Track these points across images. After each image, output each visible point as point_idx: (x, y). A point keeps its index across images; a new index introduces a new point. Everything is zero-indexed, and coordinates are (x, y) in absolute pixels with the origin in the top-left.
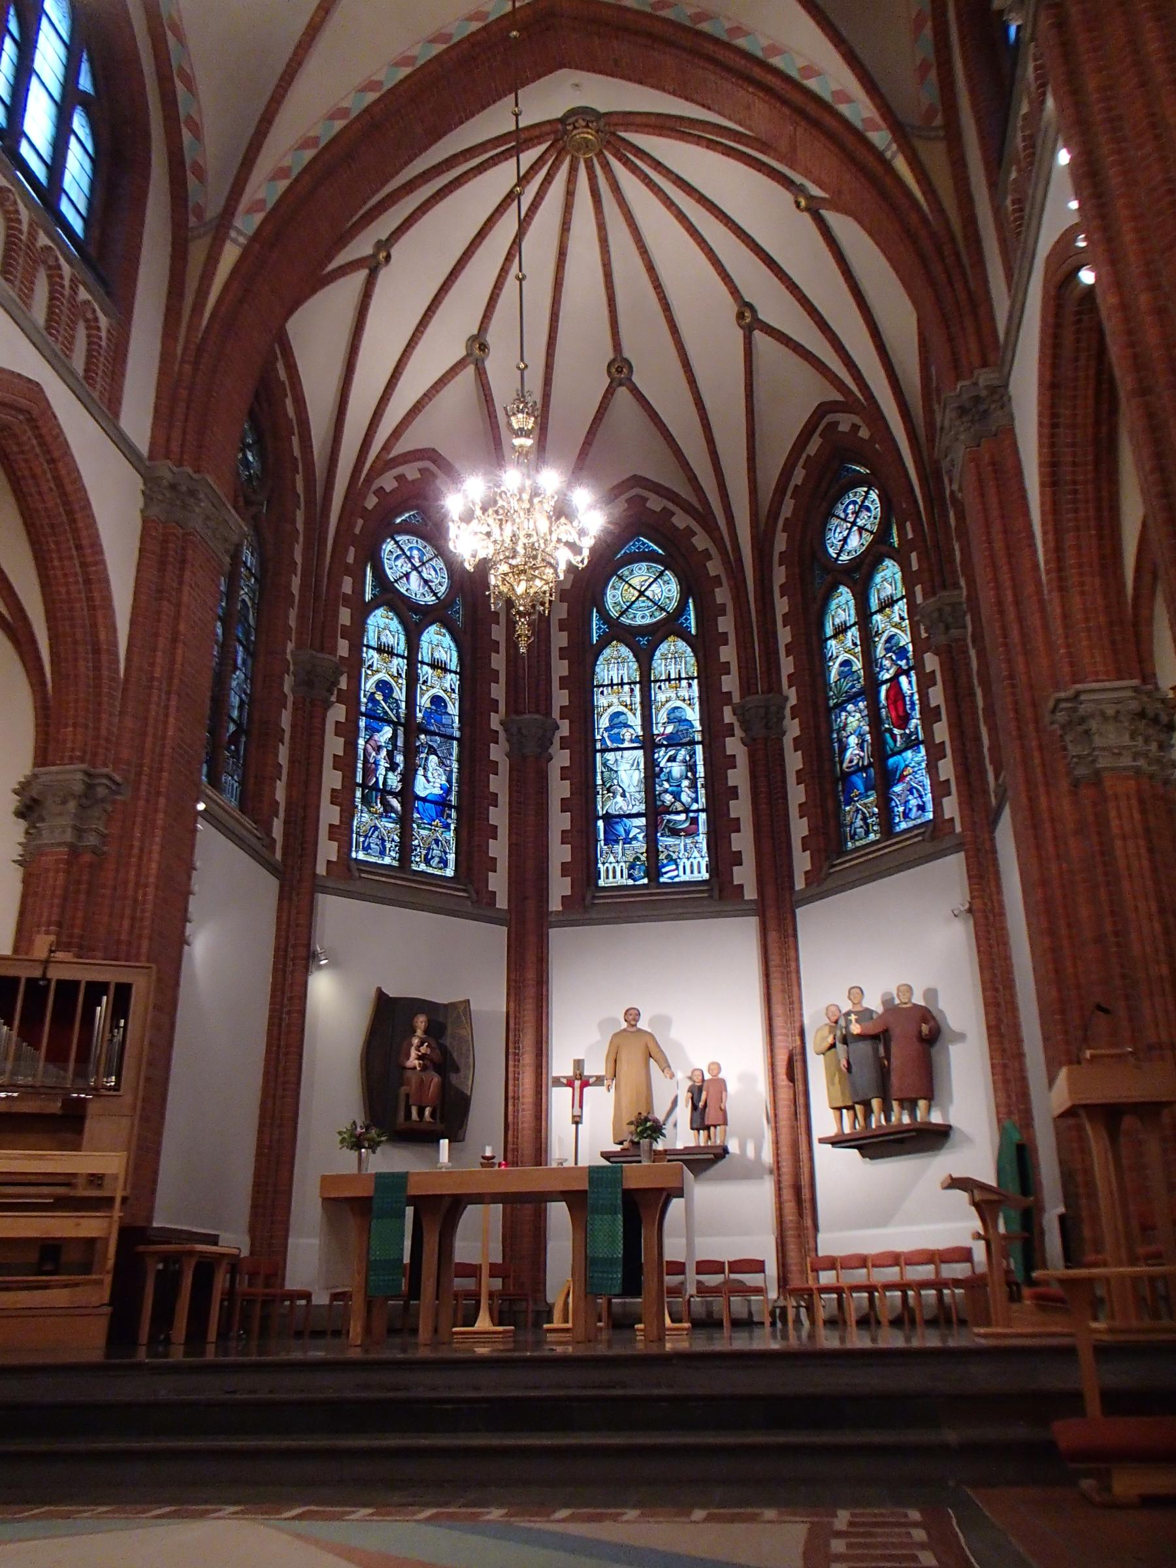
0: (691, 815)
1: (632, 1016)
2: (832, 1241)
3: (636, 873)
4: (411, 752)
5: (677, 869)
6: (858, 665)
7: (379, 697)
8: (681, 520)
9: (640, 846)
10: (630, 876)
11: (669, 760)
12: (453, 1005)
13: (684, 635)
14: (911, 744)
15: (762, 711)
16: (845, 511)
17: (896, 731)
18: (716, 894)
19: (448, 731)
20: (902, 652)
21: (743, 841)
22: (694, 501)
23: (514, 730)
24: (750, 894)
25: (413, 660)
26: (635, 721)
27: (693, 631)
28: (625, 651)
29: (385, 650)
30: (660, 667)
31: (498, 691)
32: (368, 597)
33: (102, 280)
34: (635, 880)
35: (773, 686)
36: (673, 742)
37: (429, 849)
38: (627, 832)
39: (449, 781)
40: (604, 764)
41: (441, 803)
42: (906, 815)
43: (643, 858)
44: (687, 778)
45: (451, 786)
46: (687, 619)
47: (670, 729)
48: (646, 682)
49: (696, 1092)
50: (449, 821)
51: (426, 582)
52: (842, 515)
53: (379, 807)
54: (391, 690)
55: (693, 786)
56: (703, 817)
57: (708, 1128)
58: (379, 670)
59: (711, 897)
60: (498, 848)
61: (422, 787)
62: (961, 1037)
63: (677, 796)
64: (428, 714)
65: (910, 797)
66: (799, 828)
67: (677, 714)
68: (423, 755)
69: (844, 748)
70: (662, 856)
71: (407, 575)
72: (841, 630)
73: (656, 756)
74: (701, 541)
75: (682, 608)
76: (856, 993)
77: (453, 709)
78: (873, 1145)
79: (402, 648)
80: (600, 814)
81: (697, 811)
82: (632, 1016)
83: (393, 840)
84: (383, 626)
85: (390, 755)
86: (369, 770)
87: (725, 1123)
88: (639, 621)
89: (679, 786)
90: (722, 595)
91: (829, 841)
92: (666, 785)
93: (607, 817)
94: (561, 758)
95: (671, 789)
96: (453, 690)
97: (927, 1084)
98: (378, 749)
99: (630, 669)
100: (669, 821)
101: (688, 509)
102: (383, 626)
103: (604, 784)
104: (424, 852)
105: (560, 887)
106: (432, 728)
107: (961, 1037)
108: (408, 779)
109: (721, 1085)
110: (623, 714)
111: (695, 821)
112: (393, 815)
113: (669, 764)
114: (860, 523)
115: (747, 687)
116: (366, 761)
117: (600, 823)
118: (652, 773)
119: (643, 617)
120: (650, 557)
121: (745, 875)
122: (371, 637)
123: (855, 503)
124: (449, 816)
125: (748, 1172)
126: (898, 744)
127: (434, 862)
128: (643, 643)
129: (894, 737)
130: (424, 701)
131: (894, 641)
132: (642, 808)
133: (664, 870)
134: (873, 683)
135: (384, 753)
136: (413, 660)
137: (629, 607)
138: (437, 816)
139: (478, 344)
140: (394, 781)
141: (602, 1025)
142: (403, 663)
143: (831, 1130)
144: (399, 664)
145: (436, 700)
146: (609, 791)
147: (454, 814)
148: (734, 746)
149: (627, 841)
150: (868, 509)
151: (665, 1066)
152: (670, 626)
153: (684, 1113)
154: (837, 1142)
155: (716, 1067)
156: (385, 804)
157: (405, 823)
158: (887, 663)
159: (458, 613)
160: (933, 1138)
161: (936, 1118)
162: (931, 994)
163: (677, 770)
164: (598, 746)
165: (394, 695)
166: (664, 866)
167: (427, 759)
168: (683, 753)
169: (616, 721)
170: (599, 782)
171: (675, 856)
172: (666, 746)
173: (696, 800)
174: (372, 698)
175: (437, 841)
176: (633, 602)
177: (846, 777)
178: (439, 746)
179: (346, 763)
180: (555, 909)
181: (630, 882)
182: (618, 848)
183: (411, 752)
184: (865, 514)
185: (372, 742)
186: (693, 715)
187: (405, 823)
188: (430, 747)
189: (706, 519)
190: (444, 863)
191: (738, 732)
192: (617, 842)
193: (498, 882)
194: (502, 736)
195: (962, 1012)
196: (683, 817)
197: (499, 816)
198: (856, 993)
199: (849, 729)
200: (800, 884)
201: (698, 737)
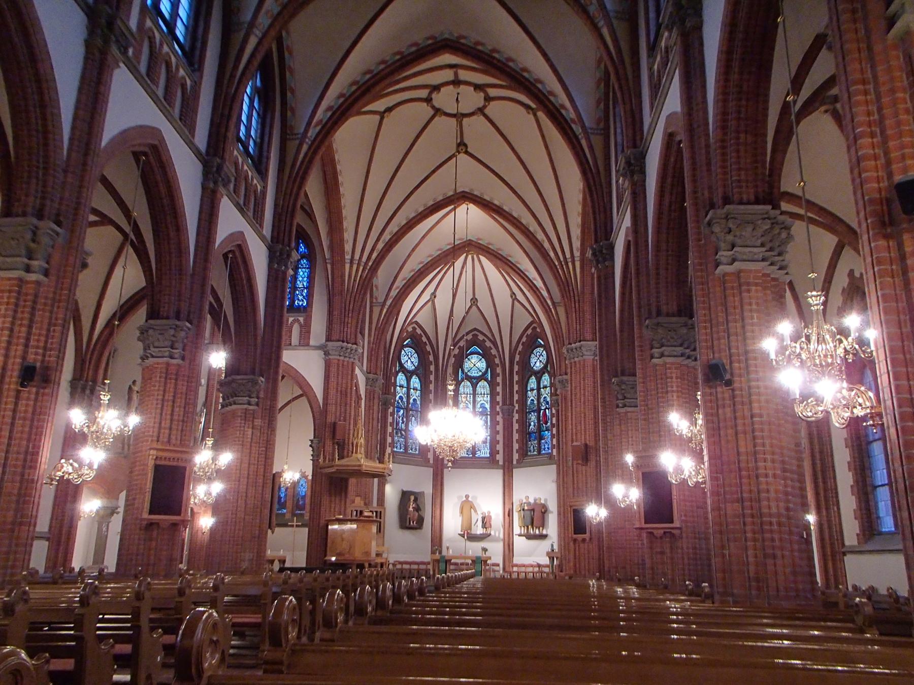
6: (535, 402)
8: (488, 344)
13: (486, 380)
14: (547, 430)
20: (547, 403)
24: (501, 463)
25: (408, 388)
28: (469, 383)
29: (401, 386)
30: (479, 389)
33: (191, 64)
49: (483, 519)
58: (401, 392)
66: (516, 446)
69: (530, 425)
72: (532, 390)
74: (494, 352)
76: (527, 497)
77: (418, 402)
78: (529, 537)
79: (405, 385)
82: (467, 496)
84: (401, 378)
86: (397, 424)
88: (473, 375)
90: (499, 370)
91: (524, 452)
97: (543, 525)
99: (469, 390)
101: (490, 340)
102: (401, 378)
109: (490, 517)
115: (504, 403)
120: (478, 353)
121: (500, 457)
125: (496, 540)
136: (408, 388)
139: (434, 295)
140: (403, 426)
141: (459, 497)
143: (519, 532)
145: (414, 400)
148: (499, 418)
151: (476, 511)
152: (483, 377)
153: (480, 523)
154: (520, 535)
155: (489, 512)
160: (543, 537)
161: (544, 532)
162: (546, 500)
177: (530, 434)
183: (407, 417)
186: (488, 406)
195: (553, 506)
198: (527, 497)
200: (515, 462)
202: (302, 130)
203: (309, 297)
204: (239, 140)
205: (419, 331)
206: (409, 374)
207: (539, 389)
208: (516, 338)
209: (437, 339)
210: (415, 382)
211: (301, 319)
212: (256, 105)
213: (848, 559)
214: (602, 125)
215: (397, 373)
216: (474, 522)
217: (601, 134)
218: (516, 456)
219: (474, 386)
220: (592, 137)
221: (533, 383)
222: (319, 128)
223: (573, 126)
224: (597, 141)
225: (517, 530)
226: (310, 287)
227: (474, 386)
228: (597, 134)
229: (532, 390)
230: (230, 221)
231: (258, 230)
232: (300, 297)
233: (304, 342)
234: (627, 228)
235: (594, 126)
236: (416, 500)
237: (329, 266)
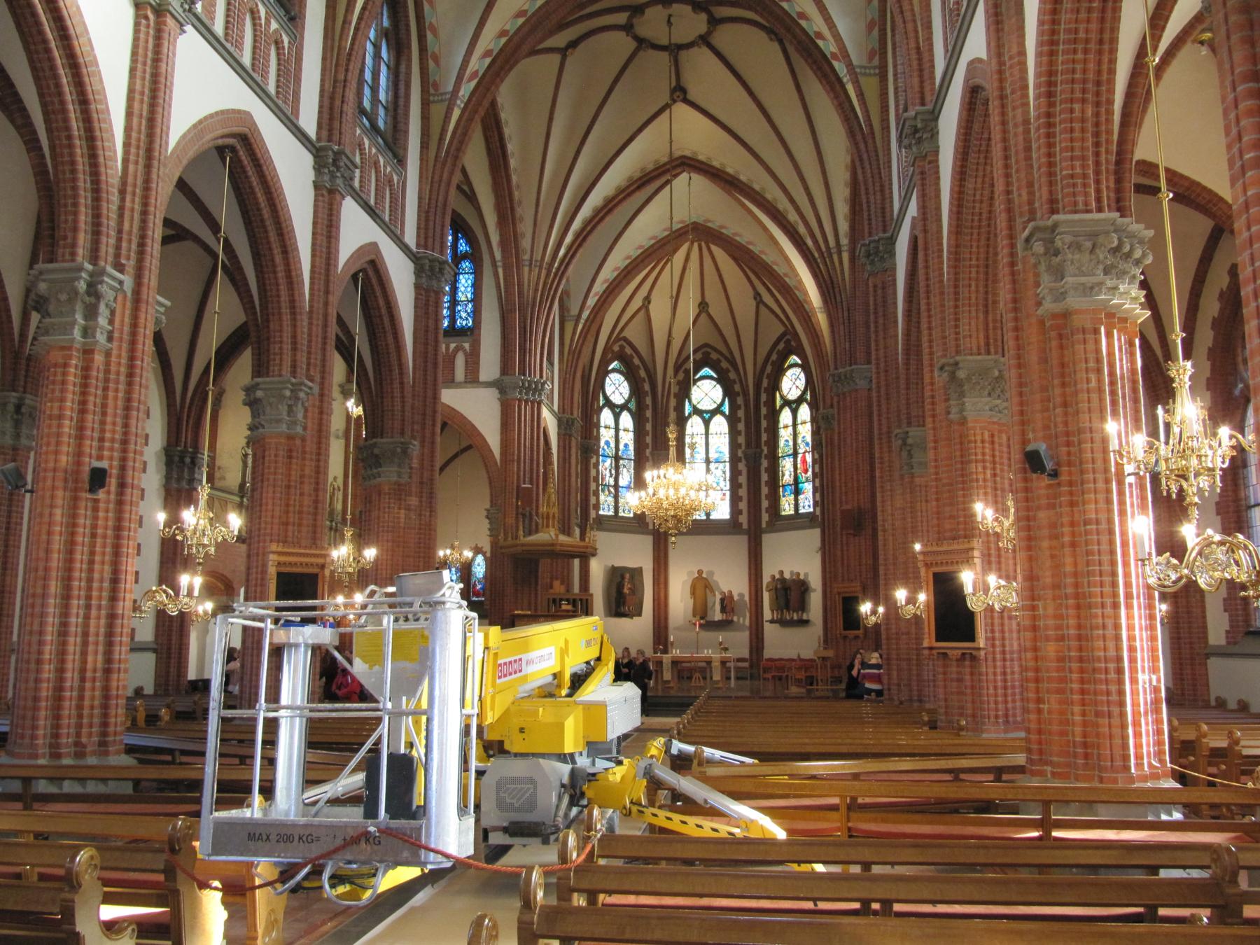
1: (700, 572)
2: (768, 653)
6: (791, 443)
13: (723, 414)
14: (807, 481)
21: (743, 505)
24: (745, 526)
25: (617, 429)
29: (607, 427)
35: (758, 445)
49: (722, 600)
56: (728, 493)
62: (815, 590)
72: (786, 427)
74: (732, 375)
76: (781, 572)
77: (631, 448)
78: (783, 623)
79: (613, 425)
90: (740, 400)
97: (802, 605)
101: (726, 358)
102: (606, 416)
107: (815, 590)
108: (616, 480)
109: (731, 597)
115: (748, 445)
120: (711, 378)
121: (743, 519)
122: (602, 424)
134: (795, 454)
136: (617, 429)
139: (647, 300)
140: (612, 482)
141: (690, 573)
144: (612, 432)
145: (626, 445)
148: (742, 466)
151: (712, 591)
152: (717, 411)
153: (718, 607)
154: (772, 622)
155: (730, 592)
157: (616, 498)
159: (632, 405)
160: (804, 623)
161: (805, 617)
162: (806, 575)
168: (721, 466)
179: (596, 479)
183: (617, 468)
191: (744, 462)
195: (815, 580)
200: (764, 525)
202: (450, 88)
203: (476, 314)
204: (362, 111)
205: (628, 351)
206: (617, 410)
207: (795, 425)
208: (763, 352)
209: (654, 361)
210: (626, 420)
211: (467, 346)
212: (384, 54)
213: (1213, 663)
214: (876, 62)
215: (601, 409)
216: (710, 605)
217: (875, 75)
218: (765, 517)
219: (707, 423)
220: (862, 80)
221: (786, 417)
222: (473, 84)
223: (836, 64)
224: (870, 85)
225: (767, 614)
226: (477, 300)
227: (707, 423)
228: (870, 75)
229: (786, 427)
230: (356, 229)
231: (399, 240)
232: (464, 315)
233: (472, 378)
234: (914, 218)
235: (864, 63)
236: (632, 577)
237: (500, 271)
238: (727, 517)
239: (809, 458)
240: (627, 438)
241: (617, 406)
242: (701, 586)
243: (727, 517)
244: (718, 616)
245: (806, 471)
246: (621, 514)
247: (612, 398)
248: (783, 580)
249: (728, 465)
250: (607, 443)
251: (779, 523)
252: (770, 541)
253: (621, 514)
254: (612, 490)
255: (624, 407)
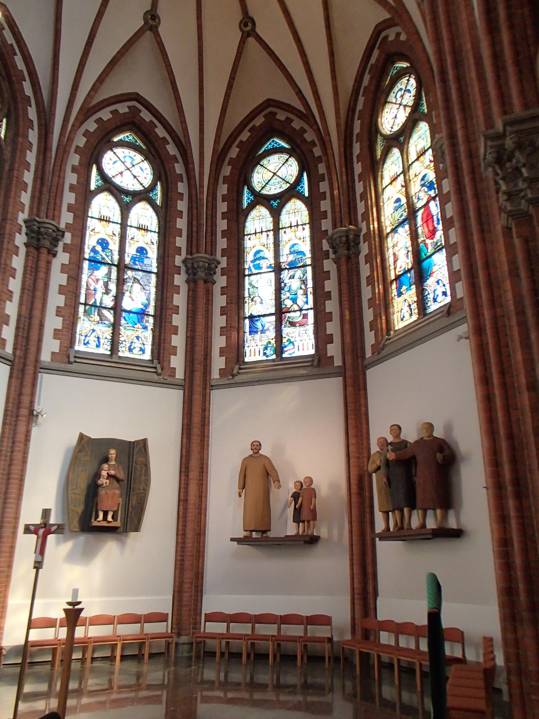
0: (304, 312)
1: (256, 446)
3: (268, 352)
4: (121, 282)
5: (294, 348)
7: (99, 248)
8: (297, 124)
9: (271, 334)
10: (265, 354)
11: (290, 278)
12: (138, 442)
13: (300, 196)
15: (344, 239)
16: (396, 97)
17: (428, 241)
18: (316, 363)
19: (149, 269)
21: (332, 328)
22: (302, 108)
23: (189, 265)
25: (124, 225)
26: (269, 254)
27: (307, 195)
30: (285, 219)
31: (181, 242)
32: (93, 187)
34: (267, 356)
36: (293, 266)
37: (132, 342)
38: (263, 326)
39: (148, 300)
40: (250, 284)
41: (142, 314)
42: (435, 300)
43: (273, 342)
44: (301, 288)
45: (149, 304)
46: (302, 187)
47: (291, 258)
48: (277, 229)
50: (147, 324)
51: (135, 177)
52: (394, 101)
53: (97, 318)
54: (107, 244)
55: (306, 294)
56: (311, 313)
57: (303, 522)
59: (312, 365)
60: (178, 341)
61: (127, 304)
63: (294, 301)
64: (134, 259)
65: (438, 287)
67: (295, 248)
68: (130, 284)
70: (284, 340)
71: (121, 173)
73: (282, 276)
75: (299, 180)
79: (117, 218)
80: (247, 316)
81: (308, 309)
82: (256, 446)
83: (106, 338)
85: (106, 285)
87: (315, 518)
89: (296, 294)
92: (288, 294)
93: (252, 318)
94: (221, 281)
95: (291, 296)
96: (153, 243)
97: (446, 497)
98: (97, 280)
100: (289, 317)
102: (104, 204)
103: (249, 297)
104: (128, 345)
105: (218, 363)
106: (136, 267)
108: (118, 298)
109: (313, 493)
110: (262, 251)
111: (305, 316)
112: (106, 322)
113: (291, 280)
114: (404, 102)
116: (88, 289)
117: (247, 321)
118: (279, 288)
119: (275, 189)
120: (279, 150)
121: (333, 350)
123: (401, 89)
124: (147, 321)
126: (429, 250)
127: (136, 351)
128: (275, 204)
129: (426, 245)
130: (131, 250)
131: (426, 179)
132: (273, 310)
133: (285, 349)
135: (101, 283)
136: (124, 225)
137: (267, 183)
138: (139, 322)
140: (108, 301)
142: (117, 229)
145: (141, 250)
146: (252, 300)
147: (151, 320)
149: (263, 332)
150: (409, 91)
152: (292, 192)
156: (100, 315)
157: (115, 326)
158: (422, 195)
161: (452, 523)
162: (448, 428)
163: (295, 284)
164: (247, 273)
165: (109, 247)
166: (285, 347)
167: (132, 286)
168: (299, 273)
169: (258, 256)
170: (246, 295)
171: (292, 340)
172: (288, 269)
173: (307, 303)
174: (94, 250)
175: (138, 338)
176: (269, 181)
178: (141, 278)
180: (215, 377)
181: (265, 358)
182: (257, 336)
183: (121, 282)
184: (407, 95)
185: (92, 277)
187: (115, 326)
188: (135, 278)
189: (307, 116)
190: (143, 351)
192: (256, 332)
193: (177, 362)
194: (183, 269)
196: (298, 313)
197: (179, 320)
199: (399, 245)
201: (309, 262)
205: (146, 116)
206: (126, 199)
209: (183, 122)
210: (143, 214)
219: (276, 214)
227: (276, 214)
238: (312, 352)
239: (435, 208)
240: (150, 241)
241: (127, 193)
242: (259, 473)
243: (312, 352)
244: (291, 529)
245: (432, 233)
246: (123, 352)
247: (117, 181)
248: (400, 445)
249: (309, 269)
250: (104, 243)
251: (392, 345)
252: (379, 380)
253: (123, 352)
254: (109, 316)
255: (143, 196)
